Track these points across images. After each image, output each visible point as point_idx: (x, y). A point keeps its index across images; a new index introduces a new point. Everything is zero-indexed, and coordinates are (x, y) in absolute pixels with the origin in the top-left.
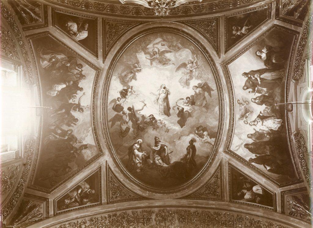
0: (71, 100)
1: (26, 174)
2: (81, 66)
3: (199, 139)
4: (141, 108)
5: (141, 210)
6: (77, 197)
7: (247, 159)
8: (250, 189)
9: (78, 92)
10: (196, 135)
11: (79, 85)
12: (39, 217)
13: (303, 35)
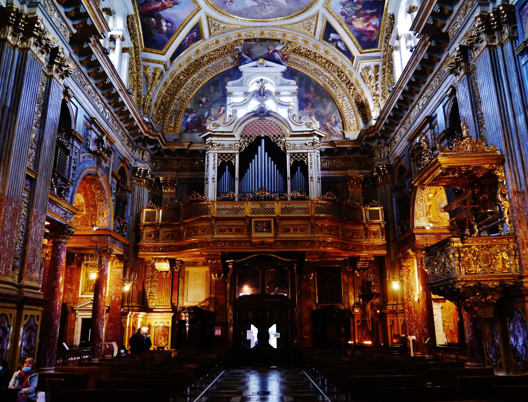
2: (342, 14)
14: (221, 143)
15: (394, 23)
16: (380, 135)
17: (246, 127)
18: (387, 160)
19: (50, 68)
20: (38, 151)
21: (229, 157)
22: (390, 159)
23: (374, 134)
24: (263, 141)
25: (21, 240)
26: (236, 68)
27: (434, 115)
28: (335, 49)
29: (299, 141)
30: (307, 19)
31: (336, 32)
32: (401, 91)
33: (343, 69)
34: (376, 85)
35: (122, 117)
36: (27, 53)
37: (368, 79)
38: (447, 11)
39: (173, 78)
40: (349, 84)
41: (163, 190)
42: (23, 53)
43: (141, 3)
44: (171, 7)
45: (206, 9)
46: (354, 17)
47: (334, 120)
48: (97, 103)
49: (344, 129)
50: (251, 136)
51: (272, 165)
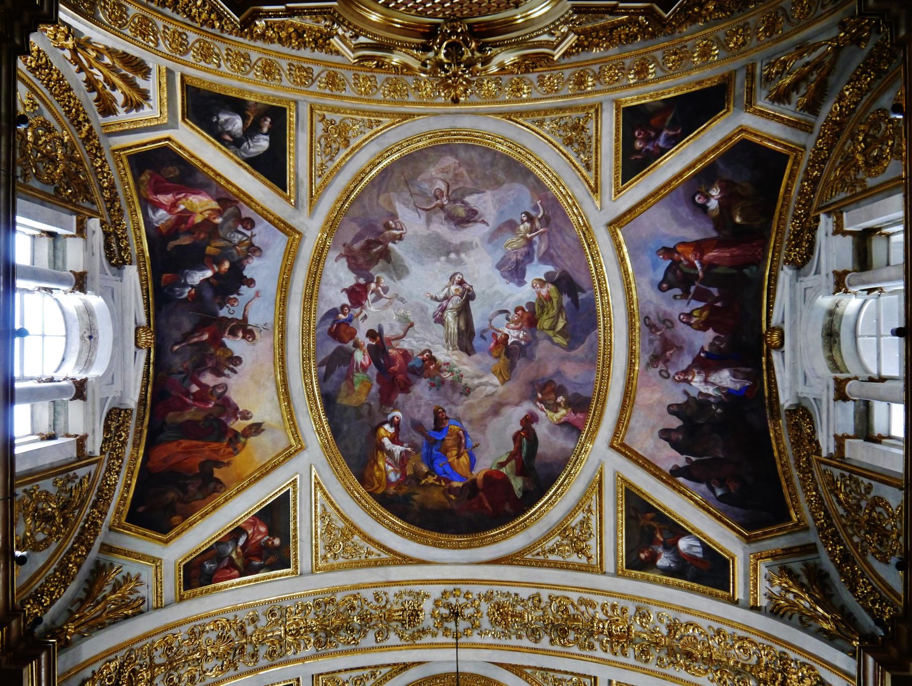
0: (225, 309)
1: (106, 494)
2: (249, 223)
3: (544, 414)
4: (401, 333)
5: (396, 589)
6: (234, 555)
7: (667, 467)
8: (671, 546)
9: (244, 288)
10: (538, 403)
12: (135, 605)
13: (813, 152)
43: (754, 268)
44: (683, 243)
46: (219, 220)
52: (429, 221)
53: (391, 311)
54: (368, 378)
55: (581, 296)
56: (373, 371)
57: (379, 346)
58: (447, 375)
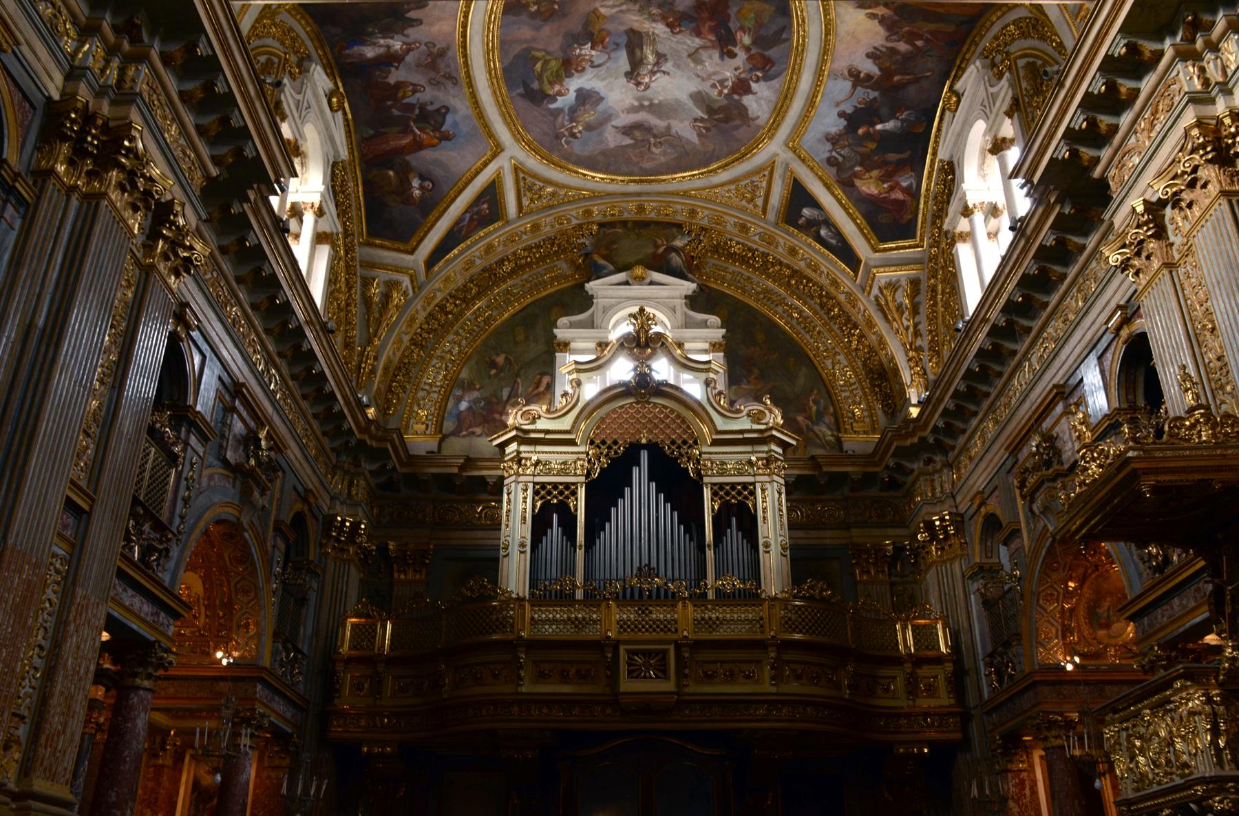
2: (831, 162)
9: (849, 111)
11: (845, 123)
14: (543, 457)
15: (953, 180)
16: (931, 440)
17: (603, 420)
18: (950, 502)
19: (149, 247)
20: (103, 445)
21: (561, 493)
22: (959, 499)
23: (916, 440)
24: (644, 455)
25: (36, 669)
26: (581, 286)
27: (1073, 381)
28: (813, 243)
29: (732, 456)
30: (748, 175)
31: (814, 203)
32: (986, 329)
33: (832, 290)
34: (916, 325)
35: (307, 390)
36: (98, 204)
37: (894, 309)
38: (1103, 127)
39: (429, 309)
40: (849, 322)
41: (396, 575)
42: (89, 204)
43: (365, 135)
44: (433, 146)
45: (514, 152)
46: (858, 169)
47: (814, 408)
48: (251, 350)
49: (839, 430)
50: (615, 442)
51: (667, 515)
52: (669, 128)
53: (710, 69)
54: (738, 20)
55: (521, 90)
56: (731, 25)
57: (725, 45)
58: (655, 11)
